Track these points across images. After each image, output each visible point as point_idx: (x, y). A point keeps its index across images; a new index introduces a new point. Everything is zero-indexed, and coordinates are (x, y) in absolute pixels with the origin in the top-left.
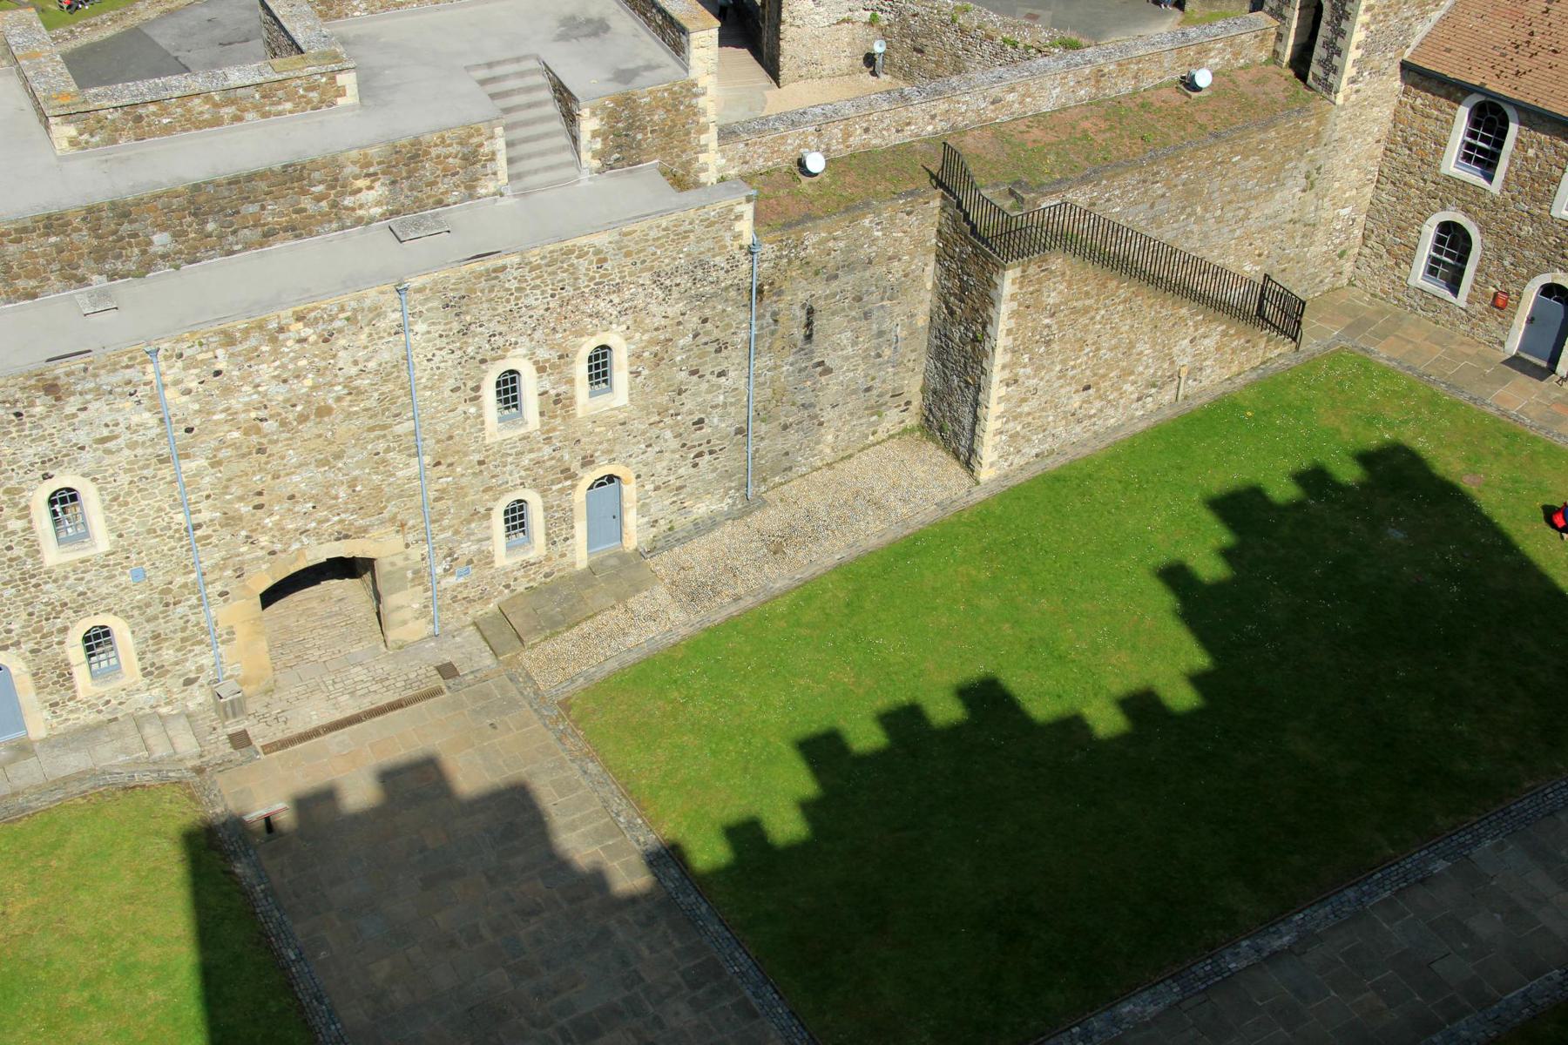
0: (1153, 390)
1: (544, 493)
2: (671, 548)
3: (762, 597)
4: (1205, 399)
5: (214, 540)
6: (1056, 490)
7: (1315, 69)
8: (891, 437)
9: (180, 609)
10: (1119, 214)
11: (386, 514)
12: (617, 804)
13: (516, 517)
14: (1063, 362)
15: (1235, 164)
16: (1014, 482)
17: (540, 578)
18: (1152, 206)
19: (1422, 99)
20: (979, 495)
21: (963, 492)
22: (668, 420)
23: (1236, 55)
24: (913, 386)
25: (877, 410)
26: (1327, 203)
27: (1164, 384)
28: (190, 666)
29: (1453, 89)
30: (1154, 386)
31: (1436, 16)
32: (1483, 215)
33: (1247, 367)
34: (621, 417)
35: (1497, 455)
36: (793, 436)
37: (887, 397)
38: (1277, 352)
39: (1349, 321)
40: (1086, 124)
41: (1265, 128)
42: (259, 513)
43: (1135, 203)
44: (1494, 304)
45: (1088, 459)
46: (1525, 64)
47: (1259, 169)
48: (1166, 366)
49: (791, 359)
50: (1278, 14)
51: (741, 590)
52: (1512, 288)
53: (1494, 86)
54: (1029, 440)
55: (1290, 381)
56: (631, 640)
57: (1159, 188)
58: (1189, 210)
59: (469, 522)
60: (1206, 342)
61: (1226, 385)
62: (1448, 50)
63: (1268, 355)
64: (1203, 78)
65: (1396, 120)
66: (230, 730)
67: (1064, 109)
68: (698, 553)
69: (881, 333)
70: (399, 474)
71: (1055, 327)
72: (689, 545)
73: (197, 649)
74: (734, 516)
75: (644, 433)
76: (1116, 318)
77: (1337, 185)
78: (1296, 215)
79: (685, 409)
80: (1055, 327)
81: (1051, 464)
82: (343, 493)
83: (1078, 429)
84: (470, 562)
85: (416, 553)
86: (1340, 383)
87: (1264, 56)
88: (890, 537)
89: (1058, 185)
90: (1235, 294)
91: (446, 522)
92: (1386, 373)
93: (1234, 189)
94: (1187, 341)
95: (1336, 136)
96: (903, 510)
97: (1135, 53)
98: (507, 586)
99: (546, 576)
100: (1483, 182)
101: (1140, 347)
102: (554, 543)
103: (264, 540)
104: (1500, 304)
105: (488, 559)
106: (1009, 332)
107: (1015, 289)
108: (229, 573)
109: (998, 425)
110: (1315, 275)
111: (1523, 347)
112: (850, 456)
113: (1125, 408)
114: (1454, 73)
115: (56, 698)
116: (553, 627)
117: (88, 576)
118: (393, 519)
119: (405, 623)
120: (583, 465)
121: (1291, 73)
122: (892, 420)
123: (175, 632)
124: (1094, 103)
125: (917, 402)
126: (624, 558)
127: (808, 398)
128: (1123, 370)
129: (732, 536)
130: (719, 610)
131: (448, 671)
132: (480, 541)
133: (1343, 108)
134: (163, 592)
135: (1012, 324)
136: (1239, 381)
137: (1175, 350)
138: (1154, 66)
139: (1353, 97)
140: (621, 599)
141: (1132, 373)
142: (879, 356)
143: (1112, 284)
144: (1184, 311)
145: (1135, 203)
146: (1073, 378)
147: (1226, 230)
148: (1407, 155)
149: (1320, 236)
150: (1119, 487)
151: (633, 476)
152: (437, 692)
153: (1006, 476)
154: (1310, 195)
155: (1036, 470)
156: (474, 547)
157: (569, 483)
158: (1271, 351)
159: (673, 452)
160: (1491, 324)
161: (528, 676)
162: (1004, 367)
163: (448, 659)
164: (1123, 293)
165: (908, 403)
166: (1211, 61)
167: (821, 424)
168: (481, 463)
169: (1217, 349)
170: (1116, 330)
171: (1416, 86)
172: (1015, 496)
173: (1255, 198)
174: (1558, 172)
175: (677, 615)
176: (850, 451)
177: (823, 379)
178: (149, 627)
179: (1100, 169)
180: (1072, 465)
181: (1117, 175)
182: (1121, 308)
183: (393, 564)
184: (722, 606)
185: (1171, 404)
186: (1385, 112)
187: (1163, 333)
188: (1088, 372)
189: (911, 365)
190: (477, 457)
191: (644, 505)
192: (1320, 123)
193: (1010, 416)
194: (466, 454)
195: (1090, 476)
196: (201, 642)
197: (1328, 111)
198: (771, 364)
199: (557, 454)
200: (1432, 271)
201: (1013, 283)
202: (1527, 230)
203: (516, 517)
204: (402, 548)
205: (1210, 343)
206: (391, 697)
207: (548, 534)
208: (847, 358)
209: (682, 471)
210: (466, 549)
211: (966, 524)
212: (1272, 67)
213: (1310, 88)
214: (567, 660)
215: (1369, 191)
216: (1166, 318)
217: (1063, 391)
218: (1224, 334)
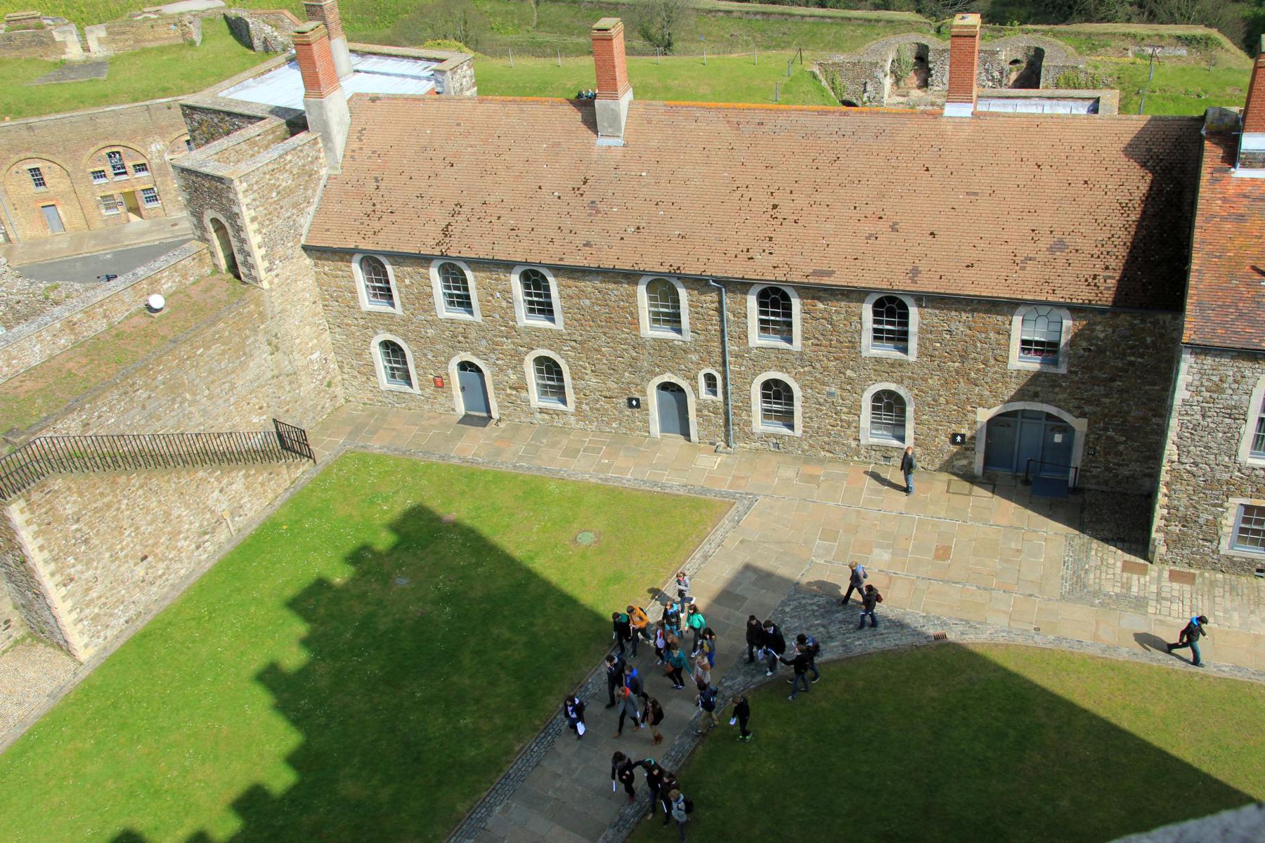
0: (207, 537)
4: (255, 526)
6: (145, 646)
7: (242, 270)
10: (117, 424)
14: (110, 549)
15: (201, 355)
16: (113, 650)
18: (144, 407)
19: (328, 266)
20: (83, 673)
23: (184, 276)
26: (296, 355)
27: (214, 529)
29: (344, 254)
30: (206, 533)
31: (312, 209)
32: (401, 330)
33: (280, 491)
35: (463, 493)
38: (301, 470)
39: (349, 429)
40: (71, 364)
41: (214, 324)
43: (126, 411)
44: (437, 386)
45: (167, 611)
46: (377, 225)
47: (224, 352)
48: (208, 515)
50: (203, 239)
52: (441, 372)
53: (362, 246)
54: (111, 615)
55: (312, 491)
57: (143, 394)
58: (179, 399)
60: (234, 487)
61: (268, 510)
62: (328, 230)
64: (157, 301)
65: (320, 285)
67: (52, 358)
71: (85, 529)
76: (141, 501)
77: (298, 341)
78: (276, 372)
80: (85, 529)
81: (140, 624)
83: (154, 589)
87: (208, 270)
89: (45, 423)
90: (256, 442)
92: (379, 459)
93: (211, 372)
95: (277, 309)
96: (18, 713)
97: (95, 301)
100: (390, 309)
101: (175, 513)
104: (440, 384)
106: (41, 548)
107: (27, 515)
109: (74, 615)
111: (468, 406)
113: (189, 558)
114: (336, 245)
121: (231, 276)
124: (77, 345)
125: (16, 618)
128: (170, 533)
133: (271, 290)
136: (278, 503)
137: (210, 503)
138: (117, 305)
139: (276, 280)
141: (180, 532)
143: (123, 479)
144: (201, 474)
145: (126, 411)
146: (126, 556)
147: (221, 401)
148: (338, 304)
149: (303, 378)
150: (194, 623)
153: (105, 649)
154: (279, 355)
158: (301, 471)
160: (441, 399)
164: (136, 480)
166: (165, 287)
169: (248, 488)
170: (147, 510)
171: (319, 259)
172: (114, 663)
173: (233, 372)
174: (428, 289)
179: (80, 395)
181: (95, 398)
182: (140, 492)
185: (229, 541)
186: (310, 281)
187: (191, 495)
188: (138, 547)
192: (258, 305)
193: (79, 606)
195: (170, 623)
197: (261, 295)
200: (393, 376)
201: (22, 511)
202: (431, 332)
211: (73, 704)
212: (217, 276)
213: (245, 283)
215: (327, 336)
217: (122, 569)
218: (247, 476)
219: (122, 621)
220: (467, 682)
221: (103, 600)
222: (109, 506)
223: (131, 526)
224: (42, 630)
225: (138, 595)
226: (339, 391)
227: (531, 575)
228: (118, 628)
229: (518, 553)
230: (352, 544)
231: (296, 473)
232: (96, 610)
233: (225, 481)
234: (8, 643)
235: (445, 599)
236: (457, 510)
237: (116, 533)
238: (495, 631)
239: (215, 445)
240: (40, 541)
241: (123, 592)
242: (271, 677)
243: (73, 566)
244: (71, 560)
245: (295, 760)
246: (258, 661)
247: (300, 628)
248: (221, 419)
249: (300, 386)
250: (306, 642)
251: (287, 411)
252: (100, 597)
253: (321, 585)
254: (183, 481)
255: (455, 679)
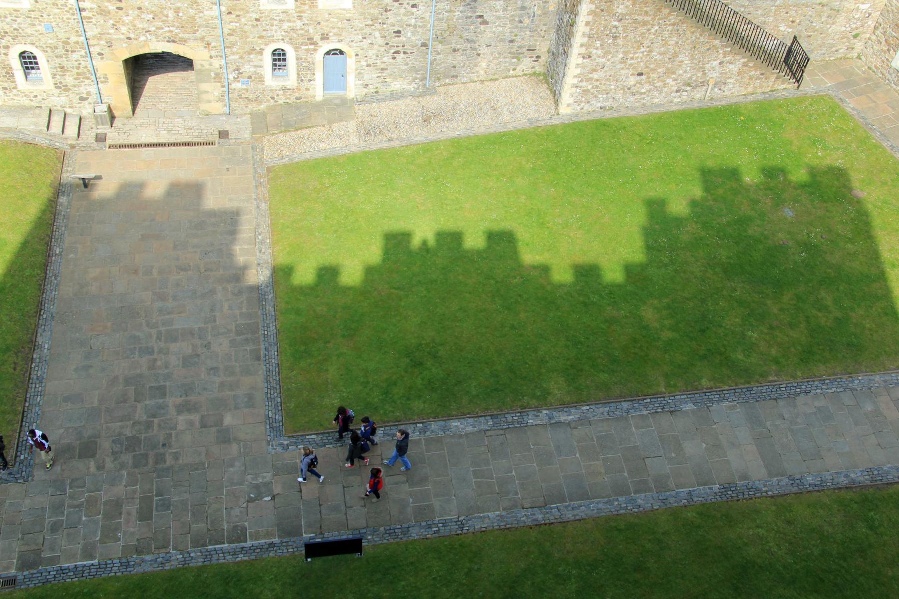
0: (688, 88)
1: (297, 49)
2: (372, 103)
3: (404, 143)
4: (723, 103)
5: (94, 20)
8: (525, 75)
9: (75, 56)
11: (198, 34)
12: (265, 229)
13: (279, 57)
14: (625, 53)
16: (581, 119)
17: (293, 99)
20: (555, 121)
21: (548, 116)
22: (378, 26)
24: (543, 47)
25: (517, 56)
27: (697, 86)
28: (83, 90)
30: (689, 85)
33: (759, 91)
34: (348, 16)
35: (884, 183)
36: (459, 58)
37: (524, 50)
42: (120, 12)
48: (699, 75)
49: (461, 8)
51: (395, 136)
54: (596, 97)
55: (780, 106)
56: (322, 146)
59: (249, 54)
60: (731, 66)
61: (741, 98)
63: (776, 87)
66: (99, 132)
68: (383, 110)
69: (523, 8)
70: (206, 13)
71: (620, 29)
72: (382, 104)
73: (87, 81)
74: (414, 95)
75: (362, 29)
79: (389, 22)
80: (620, 29)
81: (607, 115)
82: (171, 14)
83: (632, 99)
84: (250, 77)
85: (216, 63)
86: (811, 115)
88: (492, 130)
90: (770, 45)
91: (235, 50)
92: (845, 116)
94: (717, 63)
96: (506, 117)
98: (273, 98)
99: (297, 99)
101: (681, 57)
102: (302, 81)
103: (124, 29)
105: (261, 79)
106: (587, 23)
108: (103, 42)
109: (575, 81)
110: (833, 45)
112: (496, 80)
113: (667, 94)
115: (6, 85)
116: (287, 127)
117: (19, 20)
118: (202, 39)
119: (209, 102)
120: (322, 39)
122: (526, 64)
123: (73, 68)
125: (545, 58)
126: (344, 101)
127: (471, 36)
128: (668, 69)
129: (407, 105)
130: (377, 144)
131: (223, 134)
132: (255, 66)
134: (66, 43)
135: (590, 18)
136: (751, 98)
137: (707, 66)
140: (330, 122)
141: (674, 73)
142: (521, 22)
143: (666, 11)
144: (717, 42)
146: (631, 65)
149: (841, 19)
150: (638, 138)
151: (354, 54)
152: (213, 143)
153: (577, 115)
155: (596, 116)
156: (253, 70)
157: (312, 47)
159: (380, 46)
161: (262, 149)
162: (582, 45)
163: (228, 128)
164: (673, 18)
165: (538, 57)
167: (479, 55)
168: (257, 20)
169: (739, 74)
170: (665, 43)
175: (354, 139)
176: (496, 77)
177: (482, 27)
178: (58, 61)
180: (618, 120)
182: (670, 28)
183: (202, 65)
184: (380, 142)
185: (700, 101)
187: (700, 52)
188: (642, 64)
189: (542, 33)
190: (254, 16)
191: (359, 73)
193: (582, 77)
194: (248, 12)
196: (88, 78)
198: (448, 8)
199: (306, 28)
203: (279, 57)
204: (208, 58)
205: (734, 68)
206: (187, 139)
207: (298, 74)
208: (499, 18)
209: (385, 59)
210: (247, 69)
211: (537, 135)
214: (284, 147)
216: (703, 43)
217: (623, 72)
219: (599, 105)
220: (775, 311)
221: (598, 83)
222: (645, 23)
223: (648, 47)
224: (551, 78)
225: (619, 96)
226: (859, 46)
227: (881, 277)
228: (592, 108)
229: (886, 255)
230: (776, 161)
231: (780, 86)
232: (590, 87)
233: (728, 59)
234: (530, 71)
235: (808, 246)
236: (870, 193)
237: (635, 45)
238: (823, 294)
239: (742, 28)
240: (590, 18)
241: (613, 87)
242: (656, 208)
243: (597, 49)
244: (598, 44)
245: (629, 270)
246: (656, 191)
247: (698, 192)
248: (760, 12)
249: (833, 23)
250: (694, 203)
251: (809, 36)
252: (597, 80)
253: (734, 174)
254: (702, 39)
255: (769, 302)
